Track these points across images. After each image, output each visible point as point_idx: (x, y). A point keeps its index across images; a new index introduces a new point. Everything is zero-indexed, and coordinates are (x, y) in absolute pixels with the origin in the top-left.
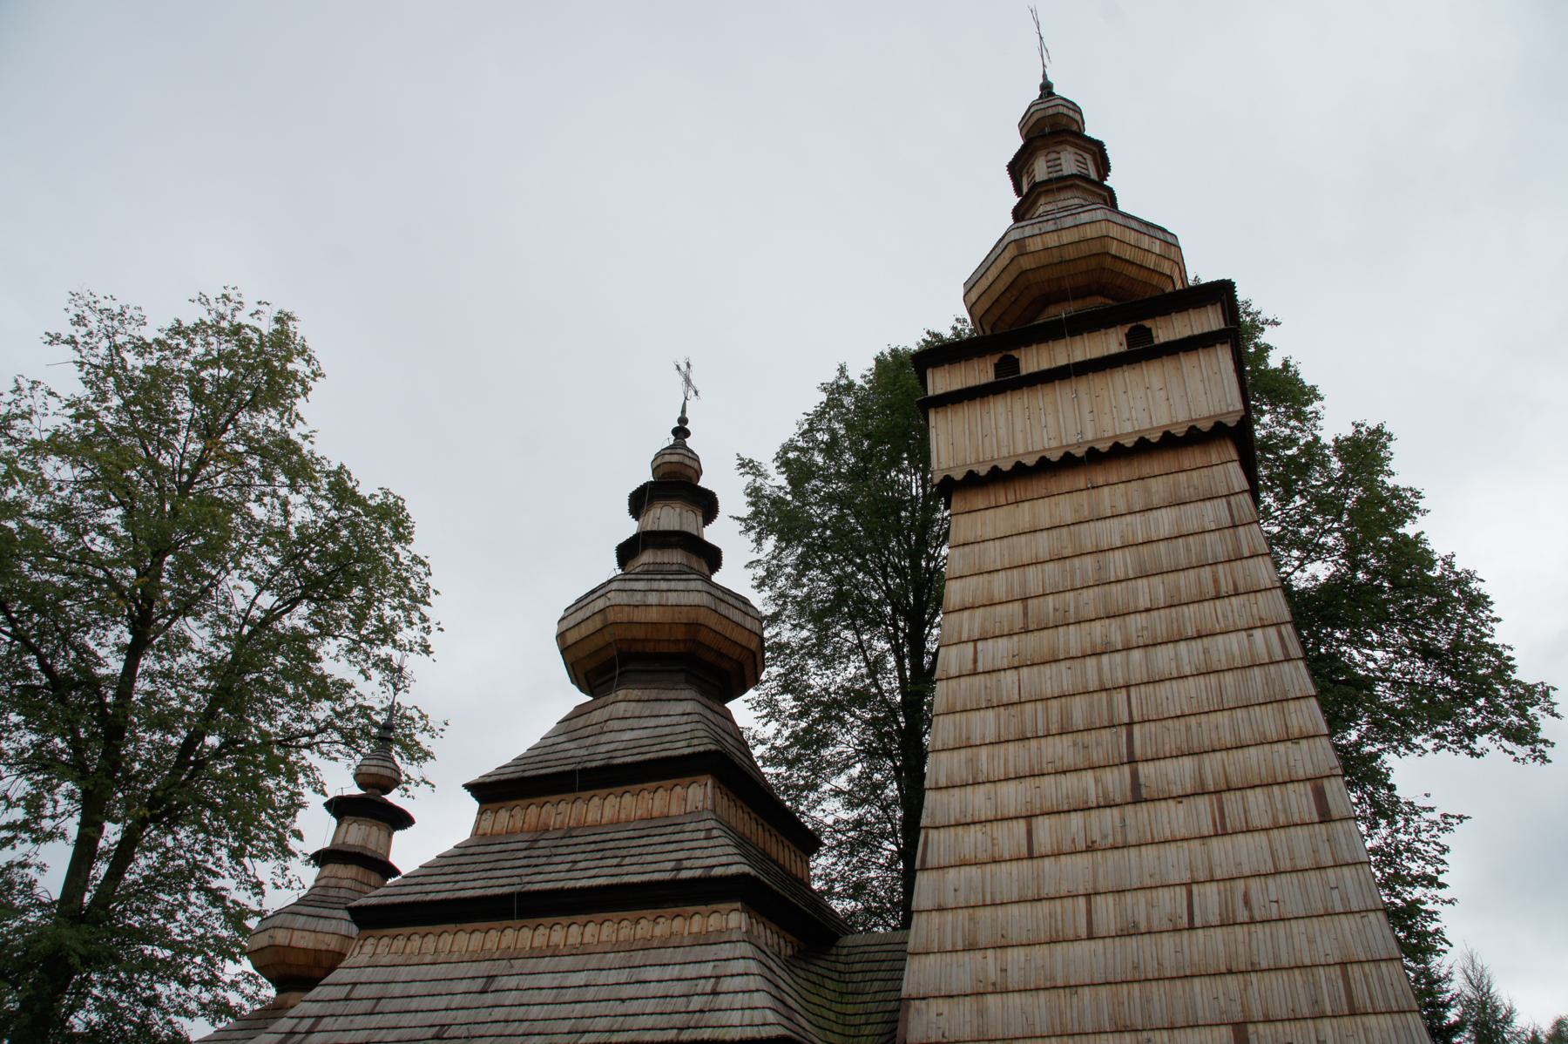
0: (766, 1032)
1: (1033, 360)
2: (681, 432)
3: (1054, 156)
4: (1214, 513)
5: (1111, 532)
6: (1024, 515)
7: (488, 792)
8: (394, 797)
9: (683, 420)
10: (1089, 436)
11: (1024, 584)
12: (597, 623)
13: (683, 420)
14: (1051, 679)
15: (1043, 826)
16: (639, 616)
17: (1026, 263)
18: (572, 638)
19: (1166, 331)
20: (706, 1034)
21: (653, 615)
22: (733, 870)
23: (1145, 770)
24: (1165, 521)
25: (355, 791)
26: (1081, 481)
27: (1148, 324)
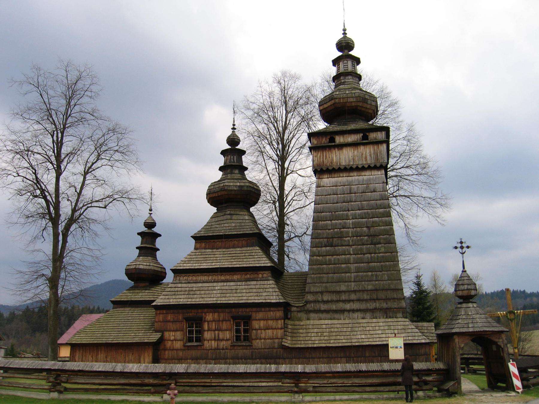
0: (281, 301)
1: (339, 140)
2: (234, 129)
3: (345, 62)
7: (197, 238)
8: (155, 230)
9: (234, 125)
10: (352, 163)
13: (234, 125)
19: (372, 136)
22: (269, 265)
27: (367, 134)
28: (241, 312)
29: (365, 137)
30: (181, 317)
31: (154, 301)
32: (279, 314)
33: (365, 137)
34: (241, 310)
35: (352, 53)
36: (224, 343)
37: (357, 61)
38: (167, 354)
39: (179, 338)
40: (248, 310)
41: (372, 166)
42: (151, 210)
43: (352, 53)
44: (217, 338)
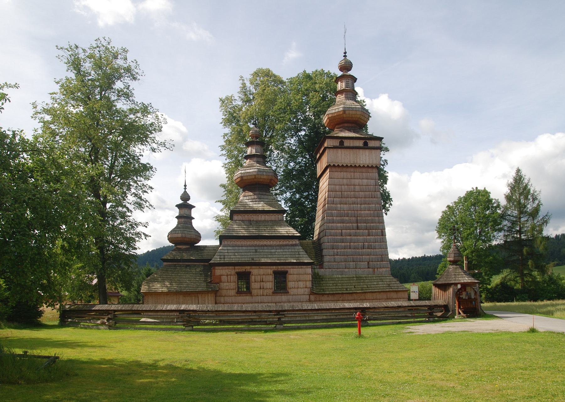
4: (373, 182)
5: (357, 181)
6: (342, 174)
11: (342, 188)
12: (253, 177)
14: (346, 207)
15: (343, 231)
16: (262, 177)
17: (345, 115)
18: (245, 178)
20: (302, 261)
21: (265, 177)
23: (359, 224)
24: (365, 181)
25: (181, 202)
26: (352, 170)
28: (280, 268)
29: (366, 144)
30: (233, 272)
31: (211, 260)
32: (309, 270)
33: (366, 144)
34: (280, 267)
35: (350, 73)
36: (268, 291)
37: (354, 79)
38: (222, 299)
39: (232, 288)
40: (285, 267)
41: (370, 166)
42: (185, 186)
43: (350, 73)
44: (262, 287)
